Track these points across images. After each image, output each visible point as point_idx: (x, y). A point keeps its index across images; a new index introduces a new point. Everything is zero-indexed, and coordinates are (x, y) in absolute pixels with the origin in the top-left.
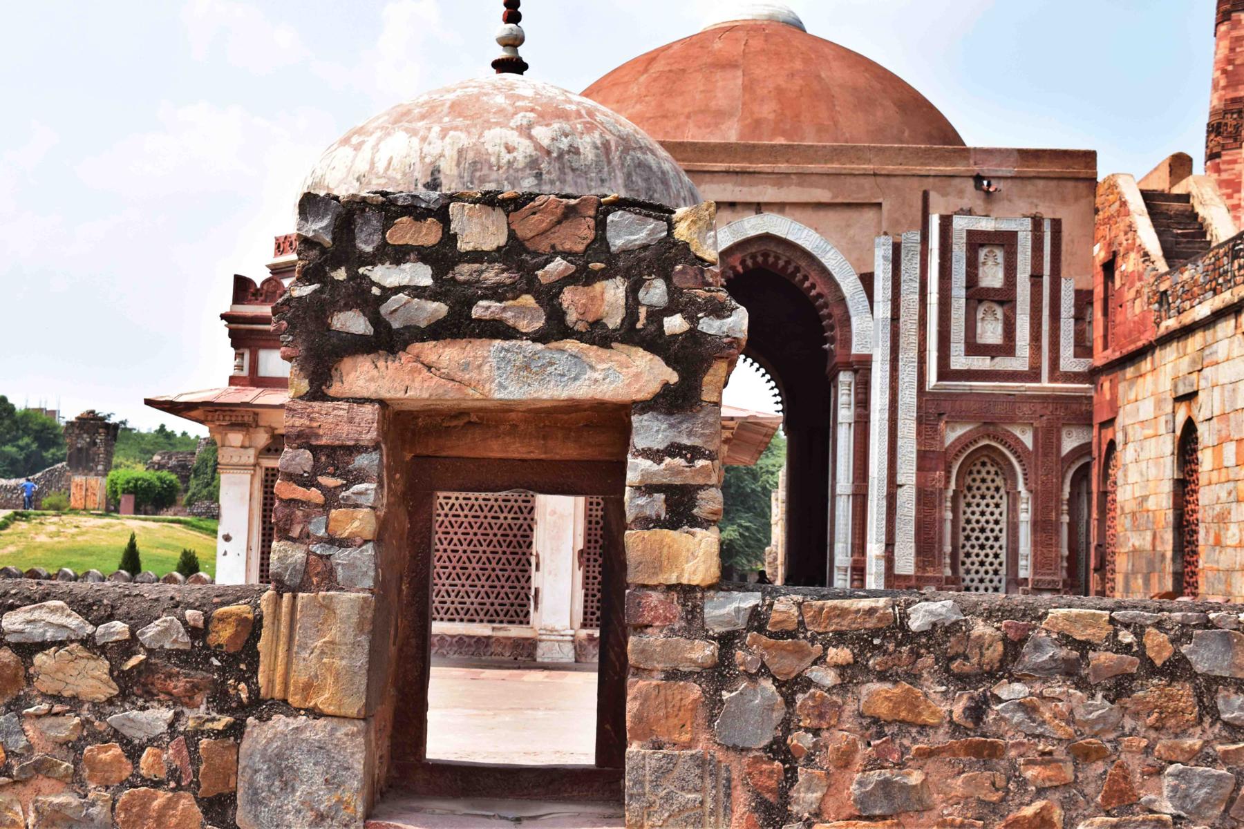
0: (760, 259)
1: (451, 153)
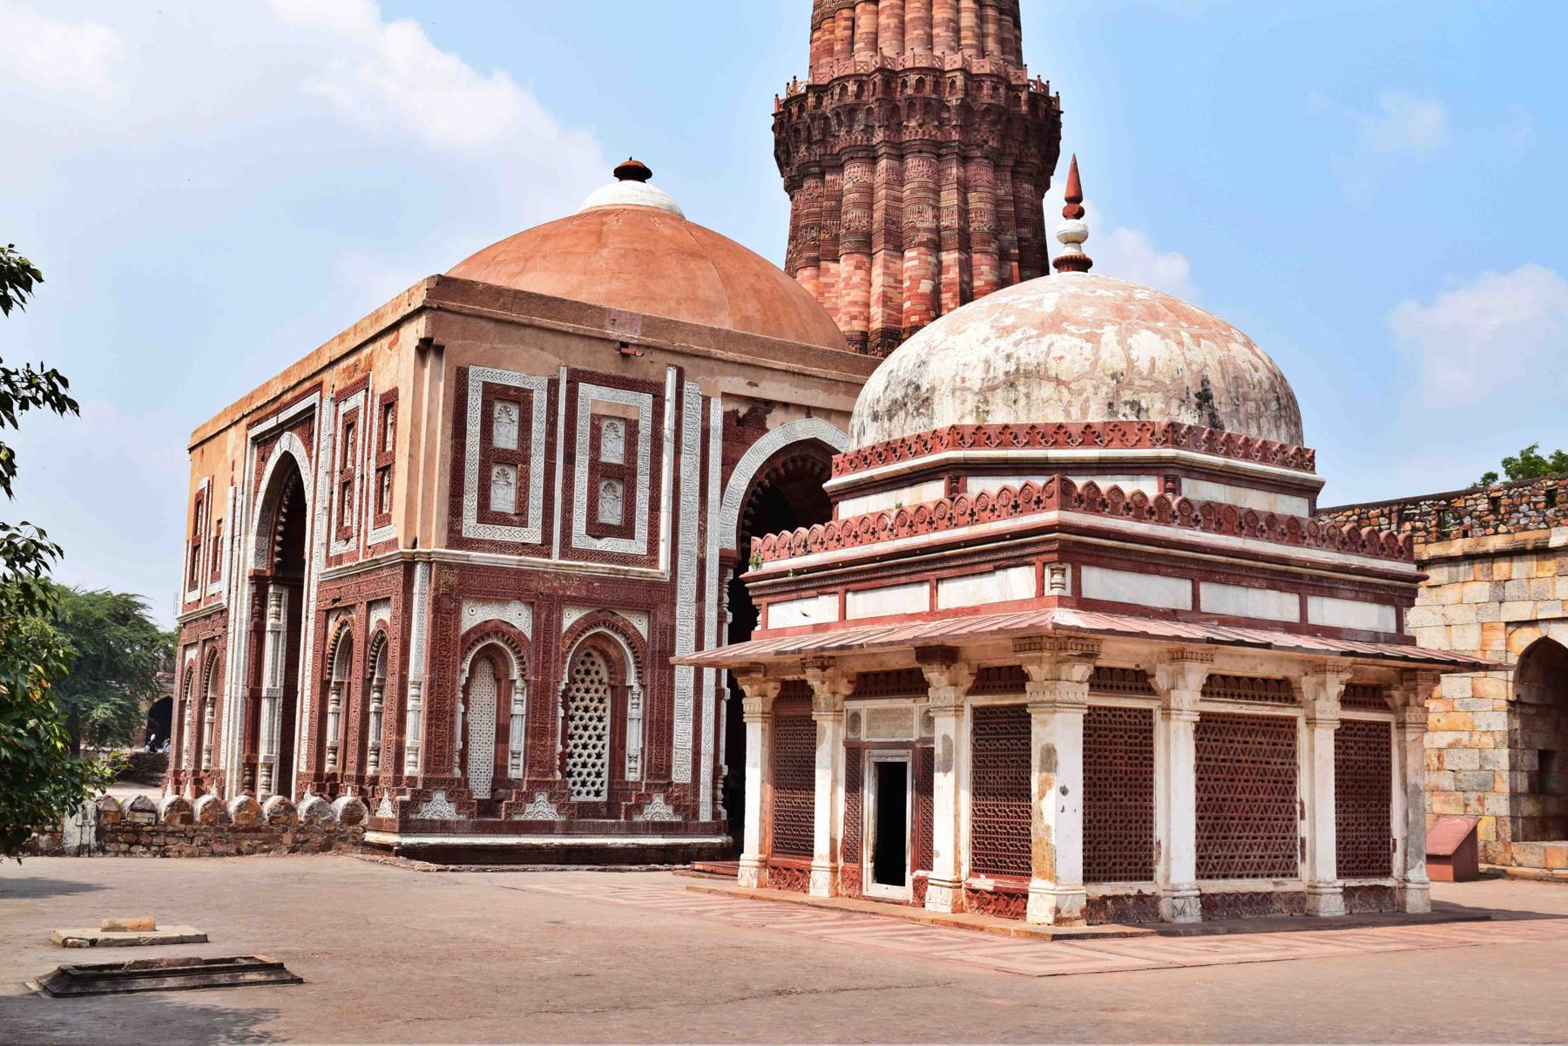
0: (799, 463)
1: (1213, 364)
